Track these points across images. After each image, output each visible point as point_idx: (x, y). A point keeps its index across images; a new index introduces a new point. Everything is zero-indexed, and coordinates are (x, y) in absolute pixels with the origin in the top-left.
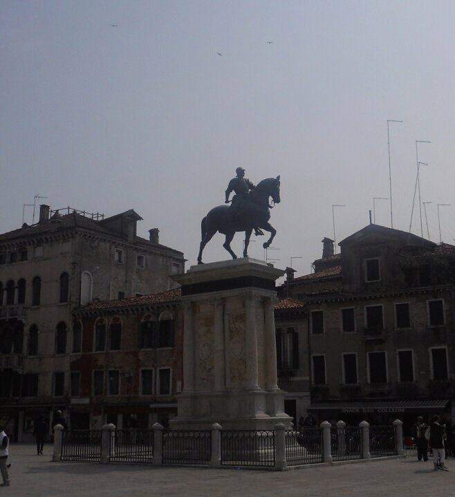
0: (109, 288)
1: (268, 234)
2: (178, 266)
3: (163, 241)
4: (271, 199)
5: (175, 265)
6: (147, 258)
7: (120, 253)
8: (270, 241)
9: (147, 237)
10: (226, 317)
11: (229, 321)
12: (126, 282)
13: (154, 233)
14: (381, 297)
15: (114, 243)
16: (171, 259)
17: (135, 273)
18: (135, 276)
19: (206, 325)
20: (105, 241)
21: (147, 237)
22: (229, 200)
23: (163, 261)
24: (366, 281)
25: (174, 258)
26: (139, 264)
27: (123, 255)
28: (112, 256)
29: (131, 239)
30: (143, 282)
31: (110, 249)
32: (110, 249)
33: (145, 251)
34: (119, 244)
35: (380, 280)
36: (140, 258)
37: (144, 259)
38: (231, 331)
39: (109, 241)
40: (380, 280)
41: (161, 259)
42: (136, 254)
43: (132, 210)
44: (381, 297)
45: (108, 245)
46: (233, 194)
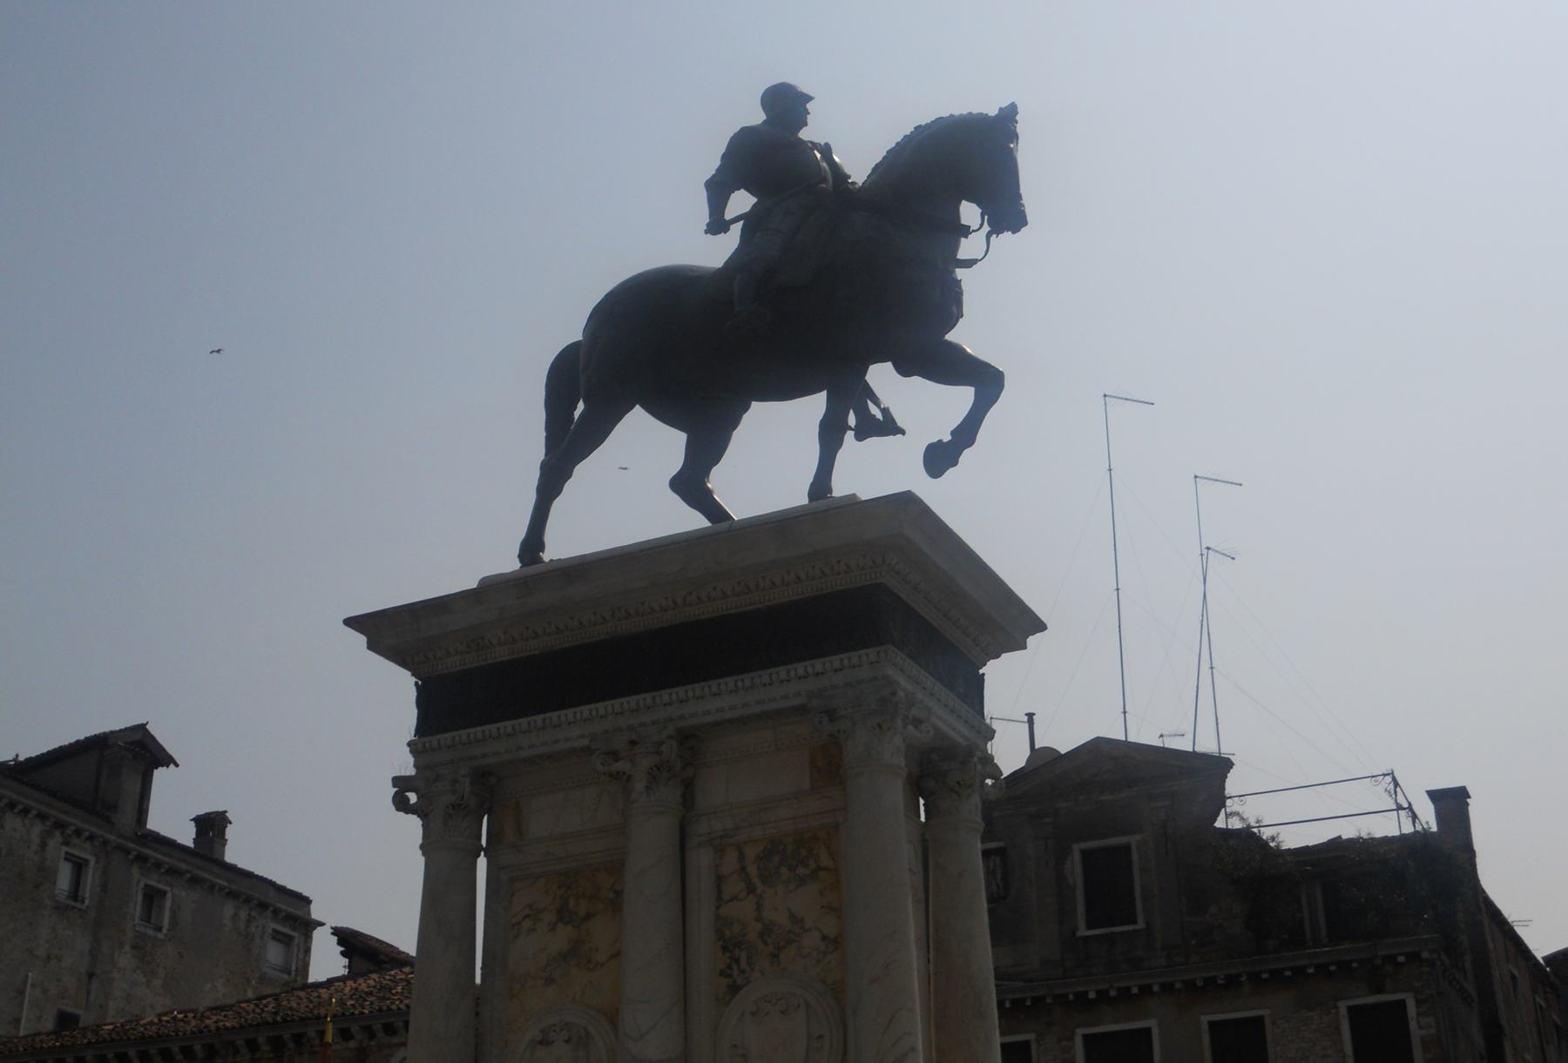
0: (21, 992)
1: (961, 398)
2: (285, 940)
3: (238, 852)
5: (278, 936)
6: (179, 897)
7: (79, 867)
8: (966, 433)
9: (186, 835)
10: (702, 860)
11: (720, 880)
12: (91, 975)
13: (212, 826)
14: (1146, 990)
15: (60, 826)
16: (269, 913)
17: (127, 948)
18: (125, 959)
19: (564, 915)
20: (26, 811)
21: (186, 835)
22: (729, 214)
23: (235, 917)
24: (1083, 932)
25: (276, 912)
26: (147, 916)
27: (91, 878)
28: (46, 874)
29: (125, 818)
30: (158, 982)
31: (44, 845)
32: (44, 845)
33: (173, 872)
34: (78, 832)
35: (1141, 925)
36: (153, 897)
37: (168, 903)
38: (730, 945)
39: (42, 817)
40: (1141, 925)
41: (229, 909)
42: (139, 880)
43: (142, 728)
44: (1146, 990)
45: (37, 829)
46: (741, 202)
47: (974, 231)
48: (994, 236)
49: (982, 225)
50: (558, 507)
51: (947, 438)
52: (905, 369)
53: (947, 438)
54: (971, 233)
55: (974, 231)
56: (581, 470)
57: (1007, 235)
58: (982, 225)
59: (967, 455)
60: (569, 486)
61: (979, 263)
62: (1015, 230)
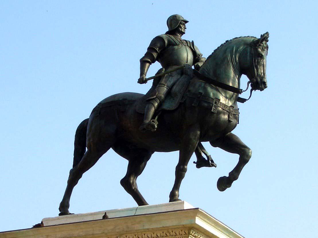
1: (235, 158)
4: (245, 79)
8: (235, 174)
46: (155, 68)
47: (244, 91)
48: (254, 91)
49: (247, 88)
50: (76, 189)
51: (227, 176)
52: (214, 144)
53: (227, 176)
54: (242, 92)
55: (244, 91)
56: (85, 175)
57: (258, 91)
58: (247, 88)
59: (234, 183)
60: (80, 181)
61: (247, 101)
62: (262, 90)
